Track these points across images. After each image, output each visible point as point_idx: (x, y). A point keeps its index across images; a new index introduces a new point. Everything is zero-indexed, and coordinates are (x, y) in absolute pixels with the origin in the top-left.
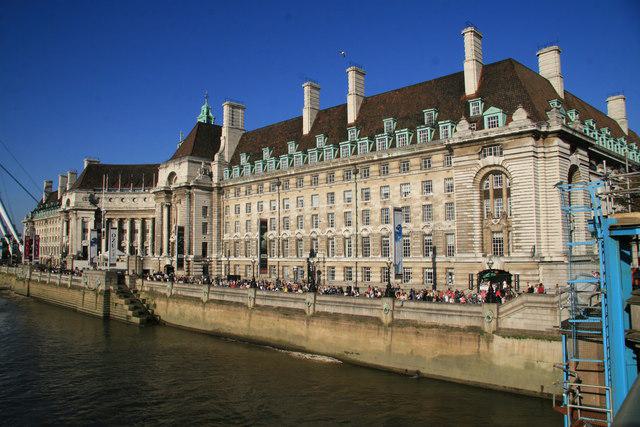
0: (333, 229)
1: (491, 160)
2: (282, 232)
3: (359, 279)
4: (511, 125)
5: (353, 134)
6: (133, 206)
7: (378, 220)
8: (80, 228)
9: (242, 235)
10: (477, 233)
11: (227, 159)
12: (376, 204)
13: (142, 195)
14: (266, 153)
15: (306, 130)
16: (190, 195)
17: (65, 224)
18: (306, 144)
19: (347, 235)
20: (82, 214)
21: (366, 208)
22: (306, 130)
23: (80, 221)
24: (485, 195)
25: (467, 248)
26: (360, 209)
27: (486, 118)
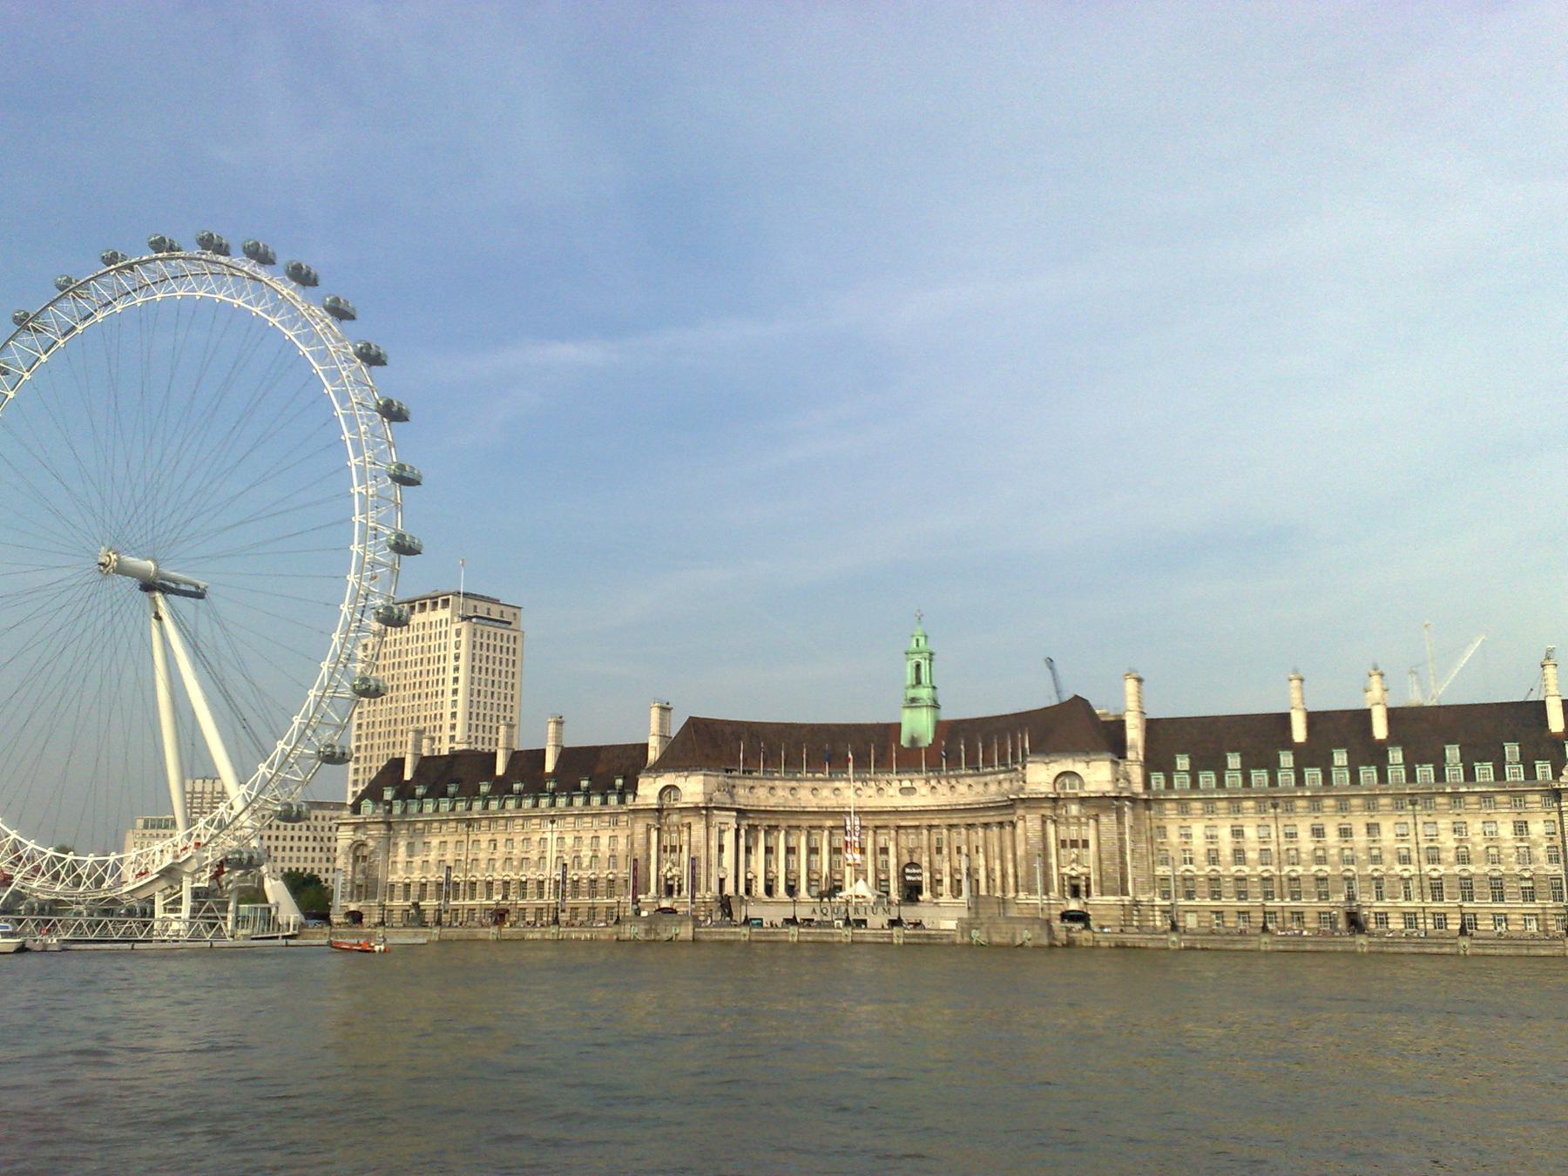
0: (1383, 868)
2: (1287, 869)
3: (1430, 927)
5: (1396, 755)
6: (793, 804)
7: (1452, 859)
8: (714, 843)
9: (1201, 869)
13: (808, 784)
14: (1234, 761)
15: (1299, 734)
16: (1120, 814)
17: (654, 835)
18: (1313, 755)
19: (1406, 874)
22: (1299, 734)
23: (714, 832)
26: (1424, 845)
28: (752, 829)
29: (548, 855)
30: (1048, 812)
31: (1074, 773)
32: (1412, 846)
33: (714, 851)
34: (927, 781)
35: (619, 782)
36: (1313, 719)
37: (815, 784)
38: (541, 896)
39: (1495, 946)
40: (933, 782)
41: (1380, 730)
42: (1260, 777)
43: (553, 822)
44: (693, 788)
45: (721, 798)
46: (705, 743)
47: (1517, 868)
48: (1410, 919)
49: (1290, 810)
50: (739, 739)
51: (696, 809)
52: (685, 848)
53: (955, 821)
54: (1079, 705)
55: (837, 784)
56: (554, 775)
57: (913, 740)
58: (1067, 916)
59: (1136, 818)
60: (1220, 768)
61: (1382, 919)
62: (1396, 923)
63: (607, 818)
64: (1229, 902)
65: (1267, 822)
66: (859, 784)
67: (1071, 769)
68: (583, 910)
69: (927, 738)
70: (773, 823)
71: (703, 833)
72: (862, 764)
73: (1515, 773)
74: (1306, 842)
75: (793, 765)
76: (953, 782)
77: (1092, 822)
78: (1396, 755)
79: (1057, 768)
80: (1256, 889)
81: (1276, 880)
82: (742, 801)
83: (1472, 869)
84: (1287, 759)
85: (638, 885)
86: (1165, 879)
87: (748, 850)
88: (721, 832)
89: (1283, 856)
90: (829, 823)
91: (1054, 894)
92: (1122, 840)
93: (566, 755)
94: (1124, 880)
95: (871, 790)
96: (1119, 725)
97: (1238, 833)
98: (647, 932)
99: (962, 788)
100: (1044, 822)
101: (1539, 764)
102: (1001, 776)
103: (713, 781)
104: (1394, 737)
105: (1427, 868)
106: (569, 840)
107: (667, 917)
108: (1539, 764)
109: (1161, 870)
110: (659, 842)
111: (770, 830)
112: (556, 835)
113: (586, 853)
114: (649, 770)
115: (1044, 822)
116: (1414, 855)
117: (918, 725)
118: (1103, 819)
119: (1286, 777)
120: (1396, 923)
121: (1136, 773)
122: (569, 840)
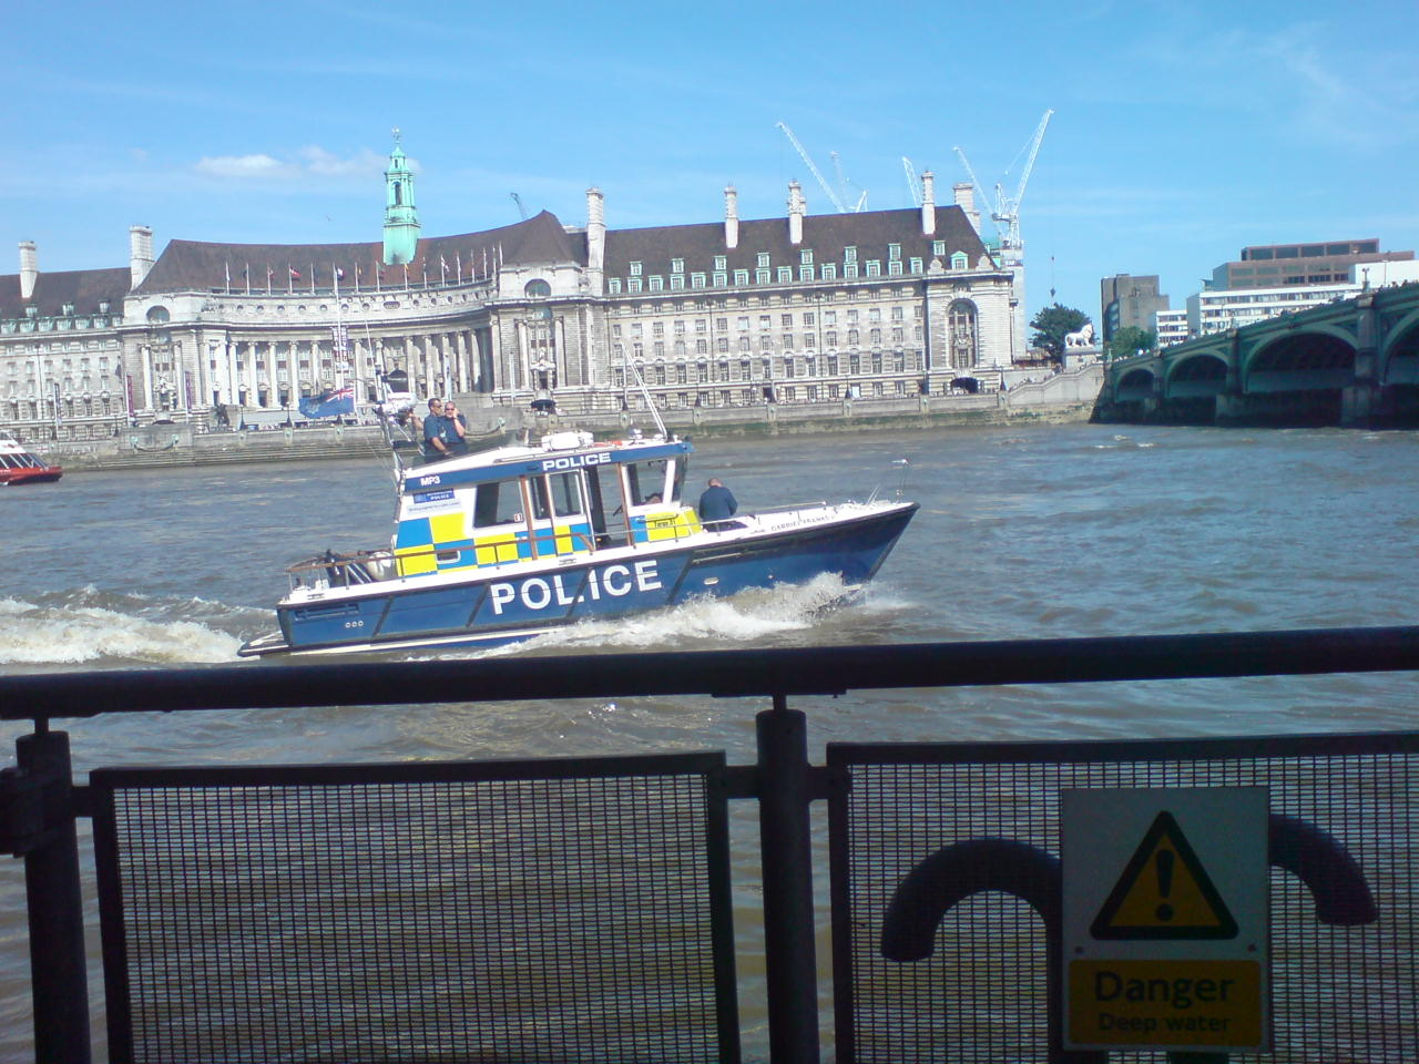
1: (962, 294)
4: (978, 269)
5: (807, 257)
6: (279, 320)
7: (845, 341)
9: (650, 359)
10: (947, 350)
11: (601, 266)
12: (843, 326)
15: (732, 240)
17: (145, 353)
18: (742, 258)
19: (810, 355)
20: (208, 336)
21: (831, 330)
22: (732, 240)
24: (952, 321)
25: (941, 362)
26: (825, 331)
27: (953, 260)
28: (243, 347)
29: (37, 378)
30: (519, 317)
31: (542, 281)
32: (816, 332)
33: (207, 365)
34: (410, 295)
35: (103, 306)
36: (744, 227)
37: (303, 302)
38: (35, 416)
39: (869, 406)
40: (415, 297)
41: (796, 236)
42: (699, 278)
43: (38, 347)
44: (181, 308)
45: (208, 317)
46: (188, 265)
47: (893, 345)
48: (811, 389)
50: (223, 261)
51: (185, 328)
52: (178, 365)
53: (436, 331)
54: (546, 219)
55: (323, 302)
56: (32, 301)
57: (395, 258)
58: (538, 405)
59: (596, 319)
60: (665, 270)
61: (790, 390)
62: (801, 395)
64: (672, 385)
65: (703, 317)
66: (344, 301)
67: (539, 277)
69: (409, 255)
70: (263, 339)
71: (195, 350)
73: (895, 267)
75: (279, 285)
76: (434, 295)
77: (558, 324)
78: (807, 257)
79: (526, 277)
80: (692, 372)
81: (709, 365)
82: (230, 319)
83: (860, 348)
84: (721, 263)
85: (135, 402)
86: (619, 371)
87: (240, 366)
88: (212, 349)
89: (716, 345)
90: (318, 338)
91: (527, 387)
92: (584, 338)
93: (43, 281)
94: (585, 373)
95: (356, 305)
96: (584, 236)
98: (147, 441)
99: (442, 299)
100: (516, 326)
101: (913, 260)
102: (478, 289)
103: (200, 302)
104: (808, 241)
105: (826, 349)
106: (58, 362)
107: (165, 426)
108: (913, 260)
109: (616, 363)
110: (151, 360)
111: (263, 347)
112: (42, 359)
113: (77, 375)
114: (135, 292)
115: (516, 326)
116: (817, 339)
117: (401, 244)
118: (567, 320)
119: (719, 277)
120: (801, 395)
121: (596, 280)
122: (58, 362)
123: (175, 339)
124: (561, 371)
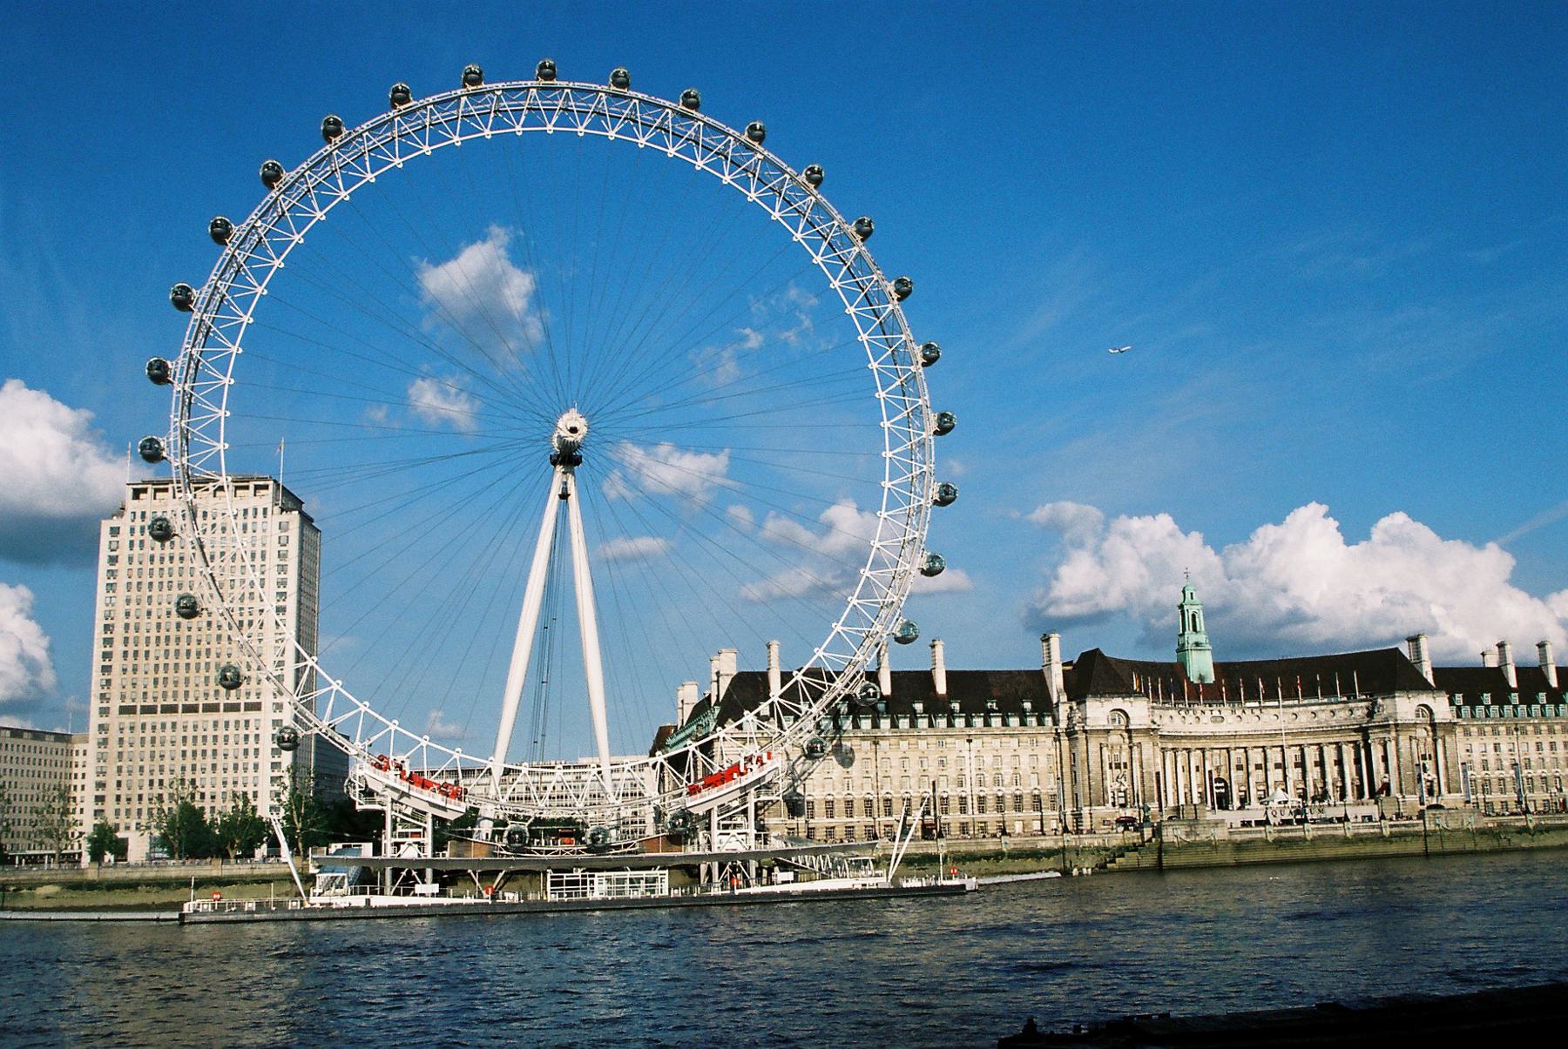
15: (1513, 683)
18: (1528, 699)
22: (1513, 683)
29: (966, 772)
34: (1233, 712)
38: (963, 811)
40: (1239, 712)
49: (1525, 733)
57: (1201, 678)
63: (1025, 738)
68: (859, 832)
69: (1211, 679)
72: (1180, 697)
74: (1534, 756)
84: (1515, 698)
95: (1190, 718)
97: (1496, 747)
98: (1187, 834)
112: (973, 754)
117: (1201, 666)
122: (989, 759)
123: (1135, 741)
124: (1443, 781)
